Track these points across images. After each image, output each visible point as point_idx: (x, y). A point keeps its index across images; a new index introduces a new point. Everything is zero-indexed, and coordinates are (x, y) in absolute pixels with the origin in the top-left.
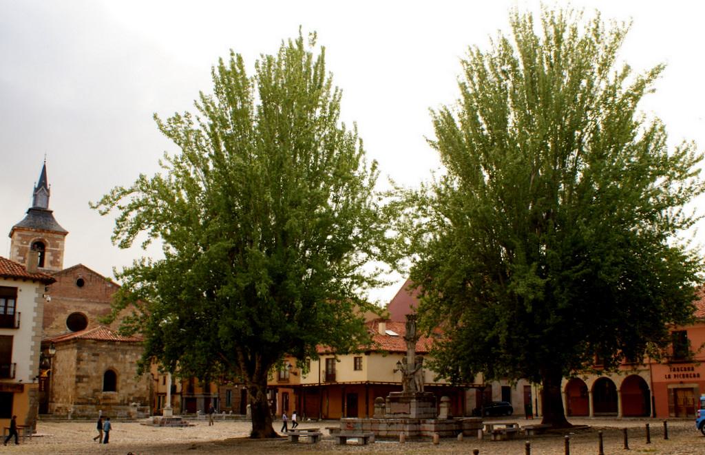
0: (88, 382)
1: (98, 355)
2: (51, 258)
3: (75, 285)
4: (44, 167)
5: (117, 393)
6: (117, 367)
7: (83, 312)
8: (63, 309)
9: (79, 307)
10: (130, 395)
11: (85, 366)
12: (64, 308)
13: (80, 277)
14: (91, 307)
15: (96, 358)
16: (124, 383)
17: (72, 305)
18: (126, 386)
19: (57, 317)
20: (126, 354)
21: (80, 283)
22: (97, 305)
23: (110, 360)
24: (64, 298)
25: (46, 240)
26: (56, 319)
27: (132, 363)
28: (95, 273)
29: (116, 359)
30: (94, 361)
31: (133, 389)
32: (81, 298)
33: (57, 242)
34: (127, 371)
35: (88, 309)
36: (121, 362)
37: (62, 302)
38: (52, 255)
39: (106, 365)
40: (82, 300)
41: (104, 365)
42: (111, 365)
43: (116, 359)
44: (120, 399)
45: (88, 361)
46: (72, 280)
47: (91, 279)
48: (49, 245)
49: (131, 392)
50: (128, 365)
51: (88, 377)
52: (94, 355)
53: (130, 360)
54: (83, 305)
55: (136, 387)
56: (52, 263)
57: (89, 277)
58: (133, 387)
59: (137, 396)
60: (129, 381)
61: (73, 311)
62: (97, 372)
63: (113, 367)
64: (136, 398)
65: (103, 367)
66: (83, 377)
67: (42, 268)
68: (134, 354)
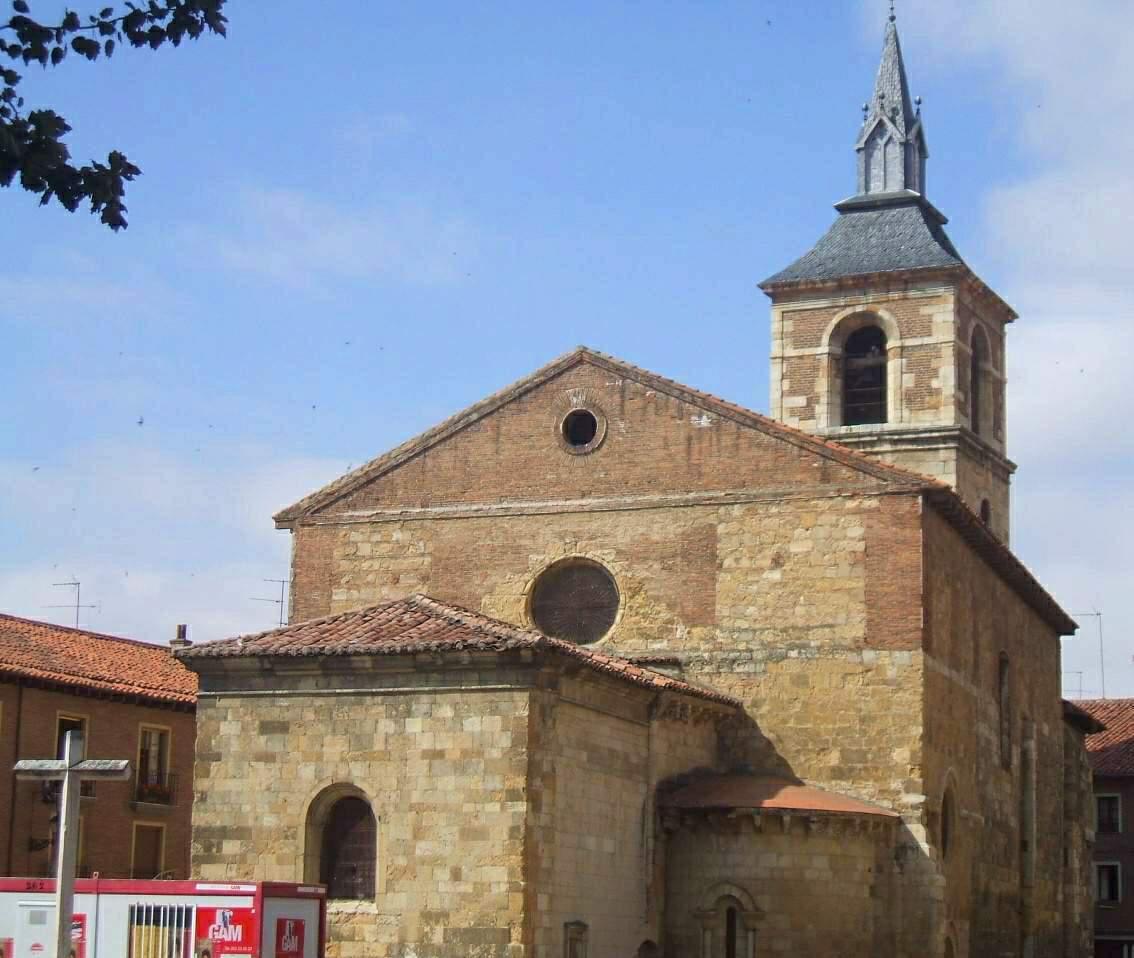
0: (242, 859)
1: (282, 728)
2: (909, 380)
5: (371, 908)
6: (375, 785)
9: (577, 536)
10: (429, 917)
11: (232, 785)
13: (577, 403)
14: (627, 530)
15: (274, 743)
16: (402, 861)
17: (546, 531)
18: (409, 872)
19: (491, 591)
20: (409, 713)
21: (580, 430)
22: (648, 515)
23: (335, 747)
25: (883, 313)
27: (439, 754)
29: (361, 746)
30: (268, 758)
31: (441, 891)
32: (583, 496)
33: (925, 311)
34: (415, 797)
35: (609, 540)
36: (386, 756)
37: (506, 524)
38: (910, 368)
39: (319, 777)
40: (590, 502)
41: (308, 772)
42: (342, 775)
43: (361, 746)
44: (385, 939)
45: (242, 758)
47: (622, 405)
48: (897, 334)
49: (435, 905)
50: (418, 768)
51: (240, 833)
52: (267, 728)
53: (426, 744)
54: (594, 525)
55: (456, 875)
56: (910, 399)
57: (617, 398)
58: (443, 875)
59: (464, 920)
60: (422, 848)
61: (555, 554)
62: (277, 809)
63: (350, 786)
64: (456, 932)
65: (307, 782)
66: (224, 833)
67: (877, 428)
68: (447, 712)
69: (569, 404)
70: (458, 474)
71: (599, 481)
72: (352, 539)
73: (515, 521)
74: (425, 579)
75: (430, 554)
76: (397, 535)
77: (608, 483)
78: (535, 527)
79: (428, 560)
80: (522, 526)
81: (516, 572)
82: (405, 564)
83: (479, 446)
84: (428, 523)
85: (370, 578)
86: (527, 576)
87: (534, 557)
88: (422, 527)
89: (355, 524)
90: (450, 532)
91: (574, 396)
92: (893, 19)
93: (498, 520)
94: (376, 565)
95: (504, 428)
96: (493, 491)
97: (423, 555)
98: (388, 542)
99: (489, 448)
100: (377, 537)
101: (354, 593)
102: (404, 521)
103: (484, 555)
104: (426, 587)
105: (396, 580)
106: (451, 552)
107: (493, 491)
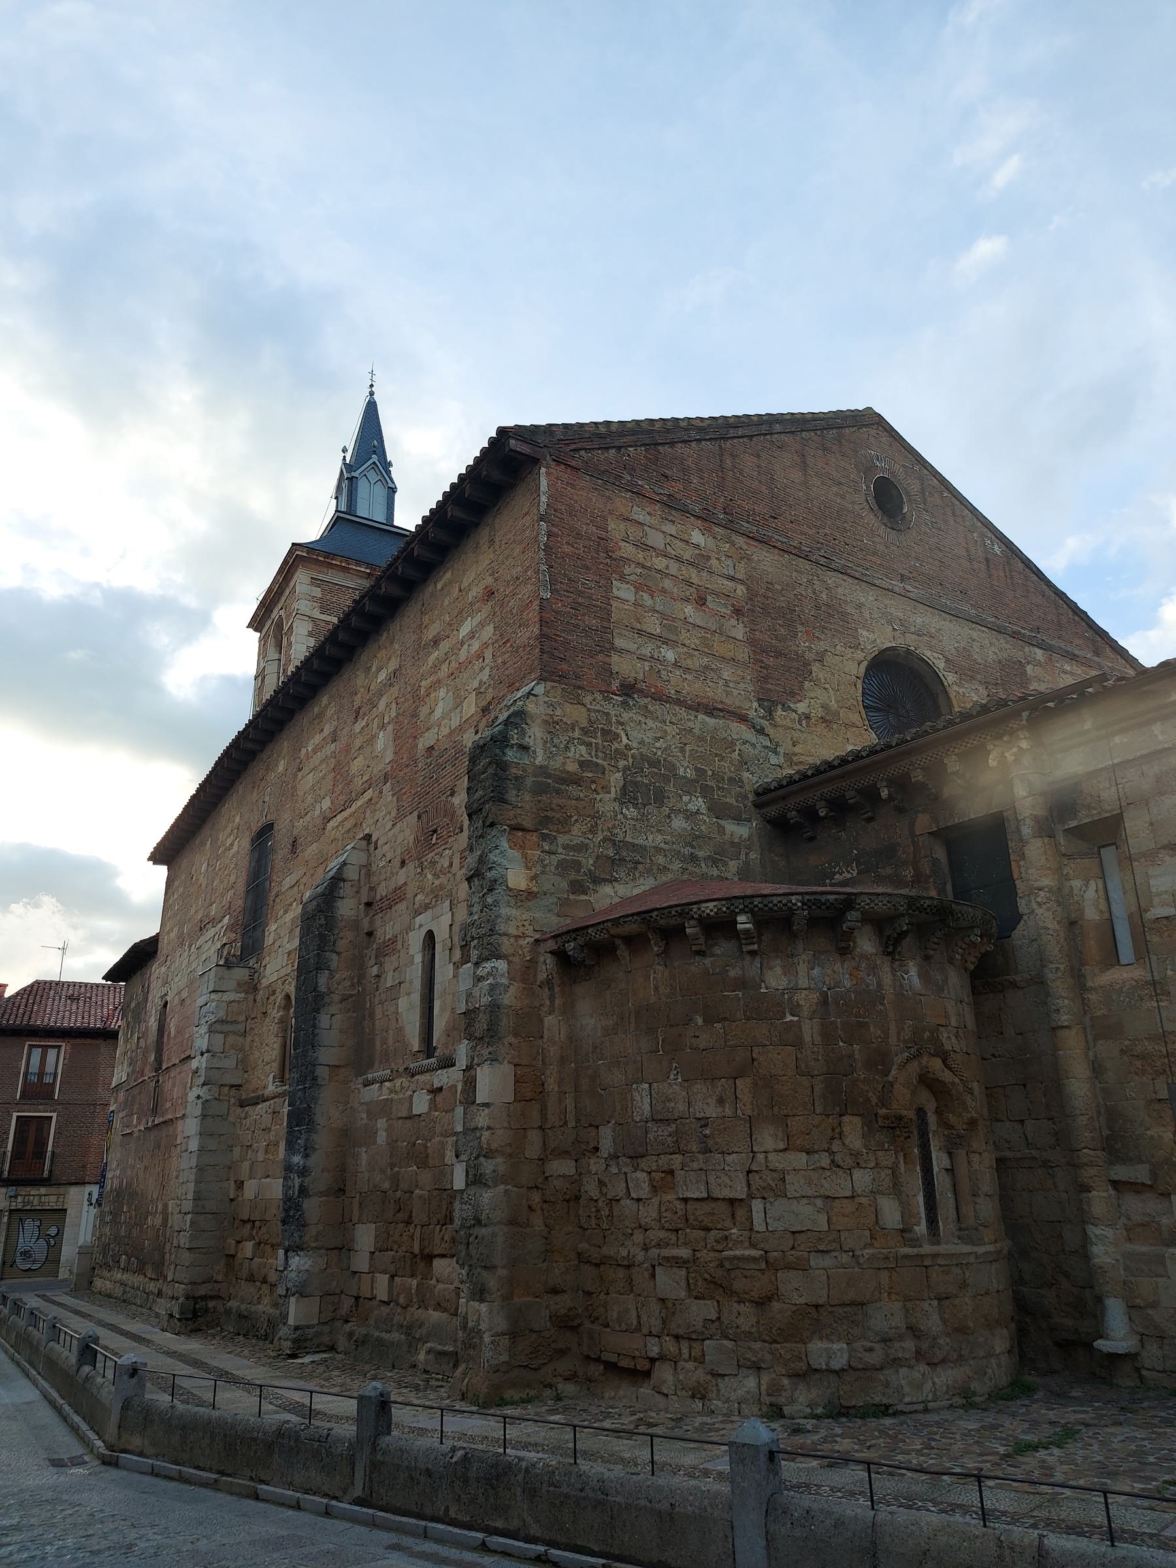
7: (928, 654)
13: (883, 469)
26: (815, 668)
37: (832, 579)
72: (636, 517)
74: (737, 612)
76: (697, 537)
85: (667, 583)
86: (859, 655)
92: (372, 386)
94: (674, 568)
97: (732, 578)
99: (797, 476)
100: (670, 529)
101: (647, 600)
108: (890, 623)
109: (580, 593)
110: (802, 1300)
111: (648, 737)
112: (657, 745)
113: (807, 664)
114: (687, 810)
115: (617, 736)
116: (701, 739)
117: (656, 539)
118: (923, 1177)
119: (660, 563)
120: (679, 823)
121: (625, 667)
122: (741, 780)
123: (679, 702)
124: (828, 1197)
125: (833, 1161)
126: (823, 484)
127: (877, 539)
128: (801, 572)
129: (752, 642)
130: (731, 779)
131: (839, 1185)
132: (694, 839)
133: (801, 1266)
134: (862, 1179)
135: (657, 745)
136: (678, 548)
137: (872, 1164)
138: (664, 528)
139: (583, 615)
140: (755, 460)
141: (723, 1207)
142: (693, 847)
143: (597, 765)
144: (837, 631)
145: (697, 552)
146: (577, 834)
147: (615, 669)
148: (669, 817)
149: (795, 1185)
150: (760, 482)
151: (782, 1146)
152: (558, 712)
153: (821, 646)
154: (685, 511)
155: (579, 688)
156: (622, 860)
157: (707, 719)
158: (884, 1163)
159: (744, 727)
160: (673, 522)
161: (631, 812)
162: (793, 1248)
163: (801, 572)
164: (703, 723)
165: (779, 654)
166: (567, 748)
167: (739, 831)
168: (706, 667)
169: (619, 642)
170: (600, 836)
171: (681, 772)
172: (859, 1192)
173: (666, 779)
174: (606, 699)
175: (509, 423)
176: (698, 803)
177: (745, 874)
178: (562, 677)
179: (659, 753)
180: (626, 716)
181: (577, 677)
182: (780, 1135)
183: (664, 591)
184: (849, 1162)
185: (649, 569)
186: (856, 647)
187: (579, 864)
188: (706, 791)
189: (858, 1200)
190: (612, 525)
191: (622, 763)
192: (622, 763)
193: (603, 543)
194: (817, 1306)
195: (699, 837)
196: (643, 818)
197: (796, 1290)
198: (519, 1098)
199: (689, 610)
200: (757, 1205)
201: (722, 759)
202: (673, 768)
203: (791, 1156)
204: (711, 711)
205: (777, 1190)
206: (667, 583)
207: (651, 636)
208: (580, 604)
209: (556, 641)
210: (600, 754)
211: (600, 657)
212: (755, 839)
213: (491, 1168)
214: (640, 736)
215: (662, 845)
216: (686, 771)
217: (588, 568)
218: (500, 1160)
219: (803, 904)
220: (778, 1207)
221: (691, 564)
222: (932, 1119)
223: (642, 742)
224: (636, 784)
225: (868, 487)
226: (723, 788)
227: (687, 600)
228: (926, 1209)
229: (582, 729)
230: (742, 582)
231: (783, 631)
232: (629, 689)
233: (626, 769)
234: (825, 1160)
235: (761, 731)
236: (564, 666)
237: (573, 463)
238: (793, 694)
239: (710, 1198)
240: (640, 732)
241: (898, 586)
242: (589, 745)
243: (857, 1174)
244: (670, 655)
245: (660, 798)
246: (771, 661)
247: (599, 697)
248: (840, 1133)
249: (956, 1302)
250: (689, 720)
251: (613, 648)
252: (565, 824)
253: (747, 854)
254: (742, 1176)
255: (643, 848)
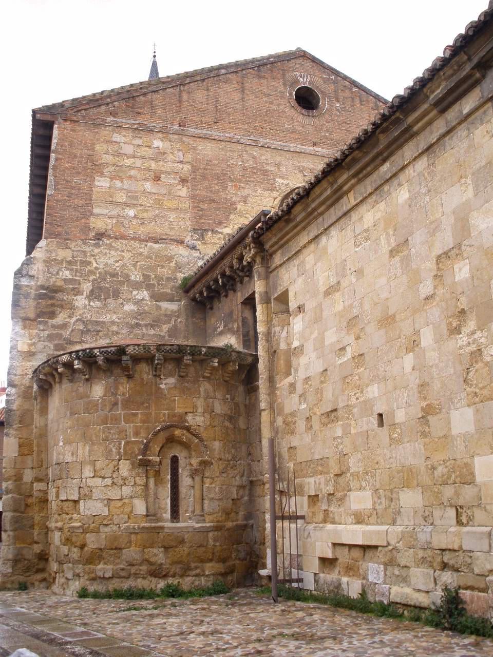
3: (294, 102)
4: (154, 65)
8: (263, 176)
12: (265, 173)
13: (304, 82)
19: (244, 200)
24: (262, 141)
26: (240, 206)
28: (345, 78)
32: (314, 144)
37: (255, 152)
46: (281, 88)
69: (297, 82)
70: (210, 107)
71: (325, 137)
72: (114, 139)
73: (263, 151)
74: (183, 181)
75: (188, 163)
76: (157, 143)
77: (332, 140)
78: (279, 159)
79: (187, 167)
80: (267, 157)
81: (265, 190)
82: (168, 167)
83: (228, 94)
84: (184, 139)
85: (133, 172)
86: (275, 194)
87: (280, 180)
88: (183, 142)
89: (118, 127)
90: (207, 149)
91: (301, 77)
92: (155, 56)
93: (248, 148)
94: (138, 163)
95: (247, 85)
96: (241, 126)
97: (182, 162)
98: (150, 147)
99: (237, 96)
100: (138, 141)
101: (118, 184)
102: (164, 131)
103: (238, 172)
104: (185, 188)
105: (157, 179)
106: (207, 164)
107: (241, 126)
108: (301, 171)
109: (73, 188)
110: (94, 547)
111: (111, 261)
112: (117, 265)
113: (233, 204)
114: (135, 299)
115: (90, 263)
116: (149, 257)
117: (128, 149)
118: (171, 491)
119: (128, 162)
120: (128, 307)
121: (98, 224)
122: (176, 278)
123: (134, 239)
124: (109, 499)
125: (113, 482)
126: (256, 97)
127: (296, 124)
128: (234, 151)
129: (193, 197)
130: (168, 279)
131: (114, 494)
132: (140, 314)
133: (97, 531)
134: (126, 491)
135: (117, 265)
136: (144, 151)
137: (132, 484)
138: (134, 142)
139: (74, 199)
140: (206, 92)
141: (71, 504)
142: (137, 319)
143: (76, 280)
144: (258, 182)
145: (157, 151)
146: (61, 318)
147: (92, 225)
148: (122, 304)
149: (96, 494)
150: (208, 104)
151: (92, 475)
152: (54, 255)
153: (246, 192)
154: (150, 131)
155: (67, 239)
156: (89, 330)
157: (156, 246)
158: (139, 483)
159: (181, 247)
160: (141, 138)
161: (98, 304)
162: (93, 523)
163: (234, 151)
164: (151, 248)
165: (213, 201)
166: (58, 273)
167: (172, 307)
168: (157, 216)
169: (96, 211)
170: (74, 319)
171: (133, 278)
172: (124, 497)
173: (122, 283)
174: (85, 243)
175: (38, 105)
176: (145, 294)
177: (173, 332)
178: (58, 235)
179: (118, 269)
180: (96, 251)
181: (67, 233)
182: (92, 470)
183: (130, 177)
184: (121, 482)
185: (121, 166)
186: (272, 190)
187: (61, 335)
188: (149, 287)
189: (124, 501)
190: (98, 147)
191: (92, 277)
192: (92, 277)
193: (90, 158)
194: (101, 549)
195: (142, 313)
196: (105, 306)
197: (93, 542)
198: (21, 454)
199: (148, 186)
200: (82, 502)
201: (163, 267)
202: (127, 276)
203: (95, 479)
204: (156, 240)
205: (88, 496)
206: (133, 172)
207: (119, 204)
208: (72, 194)
209: (55, 216)
210: (78, 274)
211: (83, 221)
212: (182, 311)
213: (5, 486)
214: (105, 261)
215: (117, 320)
216: (136, 276)
217: (79, 173)
218: (10, 482)
219: (101, 353)
220: (90, 503)
221: (152, 159)
222: (182, 462)
223: (106, 264)
224: (100, 288)
225: (291, 94)
226: (162, 284)
227: (146, 180)
228: (171, 506)
229: (68, 262)
230: (188, 163)
231: (216, 187)
232: (100, 236)
233: (94, 280)
234: (109, 481)
235: (194, 248)
236: (60, 229)
237: (75, 119)
238: (220, 223)
239: (67, 500)
240: (106, 259)
241: (310, 149)
242: (71, 270)
243: (124, 488)
244: (131, 213)
245: (117, 294)
246: (206, 206)
247: (79, 242)
248: (118, 469)
249: (177, 549)
250: (140, 248)
251: (92, 214)
252: (52, 315)
253: (176, 321)
254: (77, 489)
255: (104, 323)
